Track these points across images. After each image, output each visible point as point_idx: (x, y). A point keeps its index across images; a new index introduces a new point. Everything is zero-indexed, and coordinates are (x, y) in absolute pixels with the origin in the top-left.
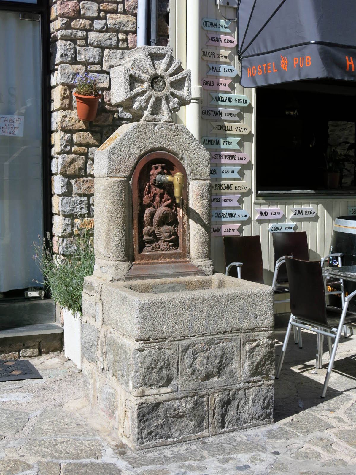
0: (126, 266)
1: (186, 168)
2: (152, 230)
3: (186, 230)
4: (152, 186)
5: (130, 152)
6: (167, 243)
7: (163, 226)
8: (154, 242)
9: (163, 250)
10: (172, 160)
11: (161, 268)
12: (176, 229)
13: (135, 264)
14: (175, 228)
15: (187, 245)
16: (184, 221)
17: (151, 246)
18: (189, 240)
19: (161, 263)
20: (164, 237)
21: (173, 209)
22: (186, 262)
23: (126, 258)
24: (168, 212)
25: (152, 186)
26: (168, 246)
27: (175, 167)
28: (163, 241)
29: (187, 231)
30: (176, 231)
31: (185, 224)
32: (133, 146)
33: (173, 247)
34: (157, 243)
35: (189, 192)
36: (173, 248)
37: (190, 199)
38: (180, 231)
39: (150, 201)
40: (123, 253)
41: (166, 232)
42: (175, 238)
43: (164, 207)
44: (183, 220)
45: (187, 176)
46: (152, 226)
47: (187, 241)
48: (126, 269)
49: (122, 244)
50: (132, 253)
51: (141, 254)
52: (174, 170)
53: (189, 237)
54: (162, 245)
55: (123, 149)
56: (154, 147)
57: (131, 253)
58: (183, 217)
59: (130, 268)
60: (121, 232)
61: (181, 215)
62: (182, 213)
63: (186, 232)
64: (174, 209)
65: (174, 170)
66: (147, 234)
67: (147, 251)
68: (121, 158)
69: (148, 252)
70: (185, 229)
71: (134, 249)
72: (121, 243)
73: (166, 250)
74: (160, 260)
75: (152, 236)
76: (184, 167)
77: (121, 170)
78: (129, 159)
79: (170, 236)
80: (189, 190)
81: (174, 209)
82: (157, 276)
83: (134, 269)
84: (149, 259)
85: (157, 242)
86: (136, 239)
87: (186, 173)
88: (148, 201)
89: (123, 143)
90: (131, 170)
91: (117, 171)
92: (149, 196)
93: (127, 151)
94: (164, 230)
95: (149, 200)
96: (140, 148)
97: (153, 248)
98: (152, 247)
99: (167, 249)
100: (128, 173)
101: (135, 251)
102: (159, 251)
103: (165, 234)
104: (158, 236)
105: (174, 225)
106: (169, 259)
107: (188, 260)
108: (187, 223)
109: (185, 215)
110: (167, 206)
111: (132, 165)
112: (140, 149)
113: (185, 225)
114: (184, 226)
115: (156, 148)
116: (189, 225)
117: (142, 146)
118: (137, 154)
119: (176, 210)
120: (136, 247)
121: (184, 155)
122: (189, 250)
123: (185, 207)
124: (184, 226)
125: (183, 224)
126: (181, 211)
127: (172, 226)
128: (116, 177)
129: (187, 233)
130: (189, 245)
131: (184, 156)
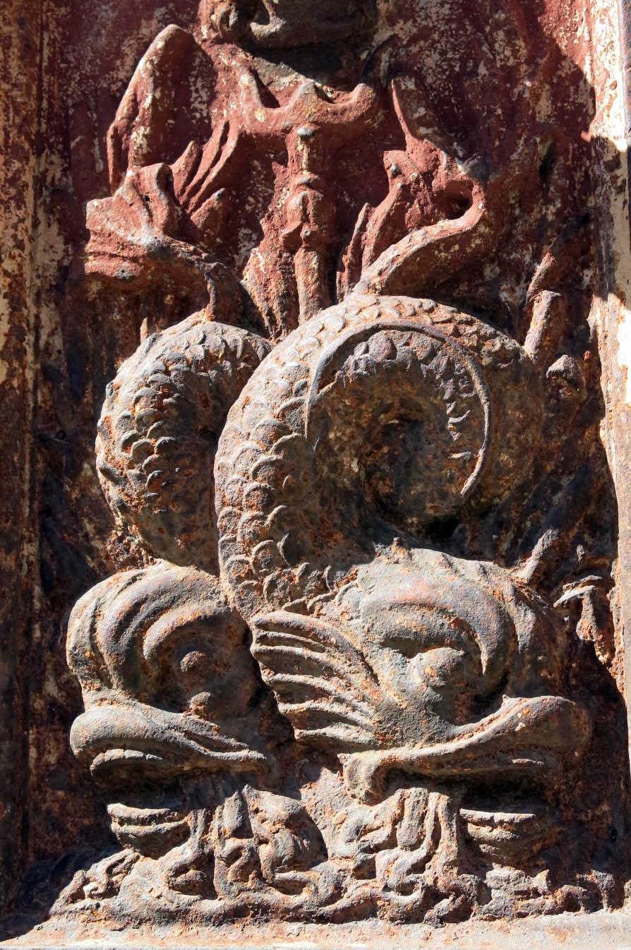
2: (185, 613)
4: (224, 57)
6: (437, 802)
7: (368, 555)
12: (576, 605)
14: (568, 595)
17: (181, 835)
20: (366, 716)
21: (515, 322)
25: (224, 57)
26: (448, 847)
28: (363, 774)
30: (585, 626)
33: (531, 871)
34: (272, 806)
36: (540, 880)
39: (178, 226)
41: (406, 645)
42: (538, 723)
43: (371, 298)
46: (213, 569)
54: (361, 831)
66: (108, 661)
67: (112, 915)
73: (412, 916)
75: (198, 698)
85: (286, 787)
94: (376, 609)
95: (161, 213)
97: (205, 861)
98: (184, 852)
99: (433, 896)
102: (295, 915)
103: (385, 662)
104: (294, 693)
105: (538, 549)
127: (509, 561)
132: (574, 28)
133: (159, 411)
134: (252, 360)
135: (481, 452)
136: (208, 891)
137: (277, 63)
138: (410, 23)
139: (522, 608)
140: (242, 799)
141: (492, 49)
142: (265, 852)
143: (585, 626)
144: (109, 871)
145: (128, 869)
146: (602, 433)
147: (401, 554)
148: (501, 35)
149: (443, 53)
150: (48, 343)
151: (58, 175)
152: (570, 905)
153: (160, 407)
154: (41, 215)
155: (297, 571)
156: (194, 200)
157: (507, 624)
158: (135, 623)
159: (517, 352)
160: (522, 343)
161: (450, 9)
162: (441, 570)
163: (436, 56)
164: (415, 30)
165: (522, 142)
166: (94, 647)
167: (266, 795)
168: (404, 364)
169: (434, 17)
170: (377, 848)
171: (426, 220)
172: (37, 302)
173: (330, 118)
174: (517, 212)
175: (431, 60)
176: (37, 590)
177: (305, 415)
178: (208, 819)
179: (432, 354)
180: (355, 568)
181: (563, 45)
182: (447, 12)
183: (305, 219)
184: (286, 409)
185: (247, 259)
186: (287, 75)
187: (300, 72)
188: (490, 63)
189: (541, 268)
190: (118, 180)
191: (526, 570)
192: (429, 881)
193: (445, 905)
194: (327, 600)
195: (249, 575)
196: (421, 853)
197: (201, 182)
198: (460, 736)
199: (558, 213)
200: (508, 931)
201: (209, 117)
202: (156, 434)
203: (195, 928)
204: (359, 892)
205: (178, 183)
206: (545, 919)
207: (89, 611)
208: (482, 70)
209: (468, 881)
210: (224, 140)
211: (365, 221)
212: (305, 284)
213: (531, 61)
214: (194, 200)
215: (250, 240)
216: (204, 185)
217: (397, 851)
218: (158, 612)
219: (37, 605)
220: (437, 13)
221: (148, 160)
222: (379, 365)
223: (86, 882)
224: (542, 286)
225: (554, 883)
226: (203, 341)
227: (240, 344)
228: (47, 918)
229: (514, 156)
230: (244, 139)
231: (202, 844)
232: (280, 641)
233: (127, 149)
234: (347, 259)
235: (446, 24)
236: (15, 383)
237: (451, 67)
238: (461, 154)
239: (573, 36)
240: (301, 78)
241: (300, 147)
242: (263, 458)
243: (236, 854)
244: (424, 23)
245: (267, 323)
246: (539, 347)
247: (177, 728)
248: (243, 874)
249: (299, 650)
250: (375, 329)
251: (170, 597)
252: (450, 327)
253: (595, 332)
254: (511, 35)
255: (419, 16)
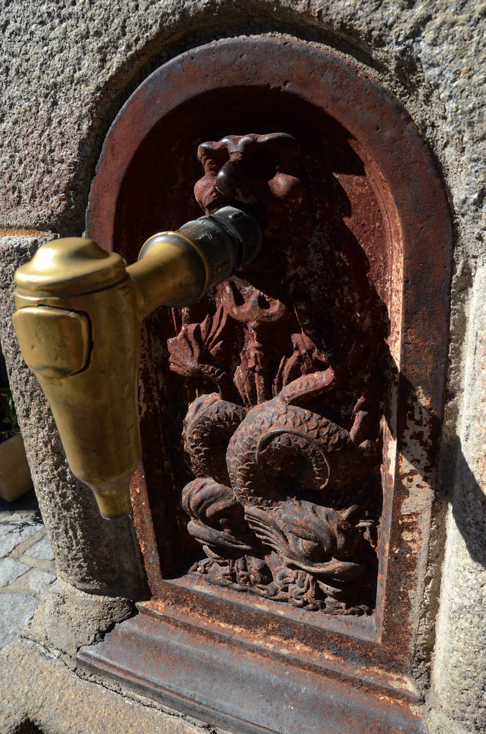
0: (95, 612)
1: (449, 155)
2: (220, 505)
3: (414, 560)
5: (48, 80)
8: (242, 553)
9: (285, 600)
10: (318, 97)
11: (241, 680)
12: (364, 529)
13: (146, 611)
14: (362, 524)
15: (416, 624)
16: (404, 511)
18: (433, 608)
19: (261, 651)
22: (392, 693)
23: (95, 585)
24: (301, 443)
26: (311, 591)
27: (364, 152)
29: (422, 561)
30: (367, 535)
31: (411, 527)
32: (58, 32)
34: (254, 563)
35: (461, 339)
37: (465, 383)
38: (384, 551)
39: (204, 358)
40: (80, 566)
44: (397, 505)
45: (452, 214)
47: (416, 610)
48: (92, 627)
49: (71, 533)
50: (136, 568)
51: (179, 582)
52: (362, 173)
53: (436, 593)
55: (15, 62)
56: (184, 13)
57: (128, 566)
58: (401, 492)
59: (111, 628)
60: (53, 486)
61: (392, 471)
62: (398, 467)
63: (412, 565)
64: (355, 428)
65: (362, 173)
67: (208, 580)
68: (16, 122)
69: (211, 583)
70: (410, 550)
71: (142, 557)
72: (62, 526)
74: (261, 632)
76: (429, 148)
77: (23, 186)
78: (50, 120)
79: (317, 555)
80: (463, 321)
81: (355, 428)
82: (203, 713)
83: (128, 636)
84: (210, 614)
86: (142, 522)
87: (445, 192)
88: (192, 364)
89: (12, 27)
90: (71, 187)
91: (13, 196)
92: (197, 331)
93: (37, 73)
94: (285, 521)
96: (98, 34)
99: (306, 603)
100: (56, 204)
101: (147, 566)
106: (306, 644)
107: (410, 686)
108: (425, 523)
109: (418, 479)
110: (299, 401)
111: (69, 153)
112: (94, 44)
113: (411, 531)
114: (407, 536)
115: (198, 13)
116: (439, 535)
117: (106, 22)
118: (84, 81)
119: (371, 431)
120: (148, 546)
121: (428, 35)
122: (429, 648)
123: (418, 436)
124: (407, 536)
125: (398, 529)
126: (391, 448)
127: (340, 507)
128: (10, 227)
129: (420, 573)
130: (432, 631)
131: (423, 48)
132: (384, 282)
133: (203, 439)
134: (236, 421)
135: (327, 480)
136: (235, 581)
137: (243, 279)
138: (304, 268)
139: (340, 535)
140: (244, 559)
141: (342, 293)
142: (252, 577)
143: (367, 535)
144: (205, 566)
145: (211, 565)
146: (381, 469)
147: (296, 503)
148: (346, 289)
149: (320, 287)
150: (162, 388)
151: (157, 318)
152: (353, 613)
153: (202, 436)
154: (152, 338)
155: (260, 499)
156: (211, 344)
157: (334, 540)
158: (202, 506)
159: (347, 437)
160: (349, 431)
161: (323, 263)
162: (311, 514)
163: (316, 288)
164: (306, 272)
165: (354, 346)
166: (190, 509)
167: (253, 558)
168: (294, 449)
169: (316, 266)
170: (289, 583)
171: (310, 371)
172: (156, 374)
173: (265, 319)
174: (351, 374)
175: (314, 289)
176: (172, 474)
177: (256, 458)
178: (234, 563)
179: (306, 446)
180: (280, 502)
181: (379, 291)
182: (322, 264)
183: (257, 363)
184: (248, 454)
185: (236, 369)
186: (248, 286)
187: (254, 286)
188: (341, 301)
189: (360, 401)
190: (179, 329)
191: (345, 514)
192: (305, 599)
193: (310, 606)
194: (271, 509)
195: (242, 494)
196: (303, 590)
197: (213, 336)
198: (316, 567)
199: (369, 379)
200: (330, 619)
201: (215, 301)
202: (202, 446)
203: (231, 591)
204: (282, 596)
205: (203, 336)
206: (344, 617)
207: (187, 494)
208: (337, 303)
209: (318, 602)
210: (221, 317)
211: (284, 366)
212: (259, 389)
213: (361, 300)
214: (211, 344)
215: (237, 361)
216: (214, 338)
217: (295, 585)
218: (210, 504)
219: (173, 479)
220: (317, 264)
221: (190, 321)
222: (284, 447)
223: (198, 567)
224: (362, 407)
225: (347, 607)
226: (217, 413)
227: (232, 414)
228: (187, 574)
229: (350, 353)
230: (229, 318)
231: (232, 570)
232: (252, 519)
233: (181, 315)
234: (276, 380)
235: (321, 271)
236: (151, 410)
237: (324, 295)
238: (325, 347)
239: (384, 286)
240: (254, 289)
241: (253, 331)
242: (241, 467)
243: (242, 576)
244: (310, 269)
245: (244, 402)
246: (356, 436)
247: (221, 537)
248: (245, 581)
249: (261, 524)
250: (283, 432)
251: (214, 497)
252: (316, 432)
253: (382, 430)
254: (351, 290)
255: (308, 265)
